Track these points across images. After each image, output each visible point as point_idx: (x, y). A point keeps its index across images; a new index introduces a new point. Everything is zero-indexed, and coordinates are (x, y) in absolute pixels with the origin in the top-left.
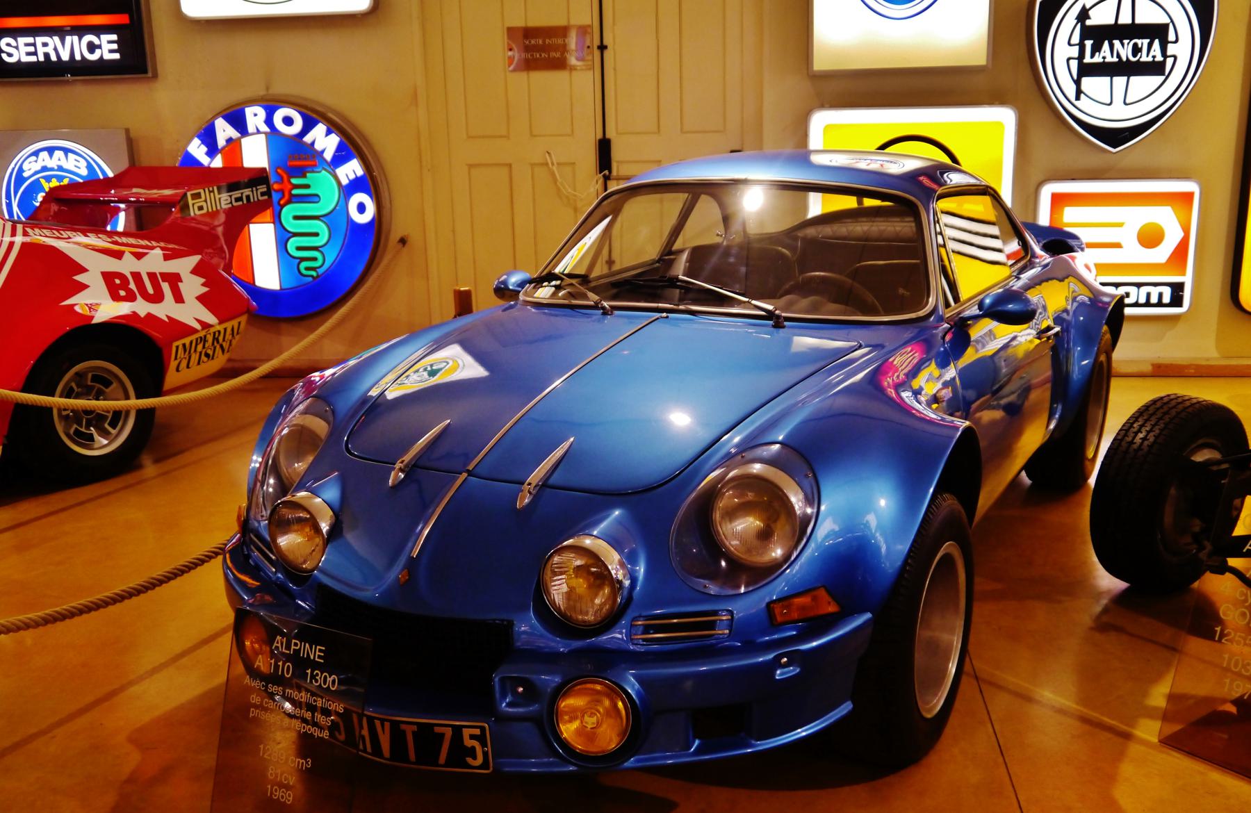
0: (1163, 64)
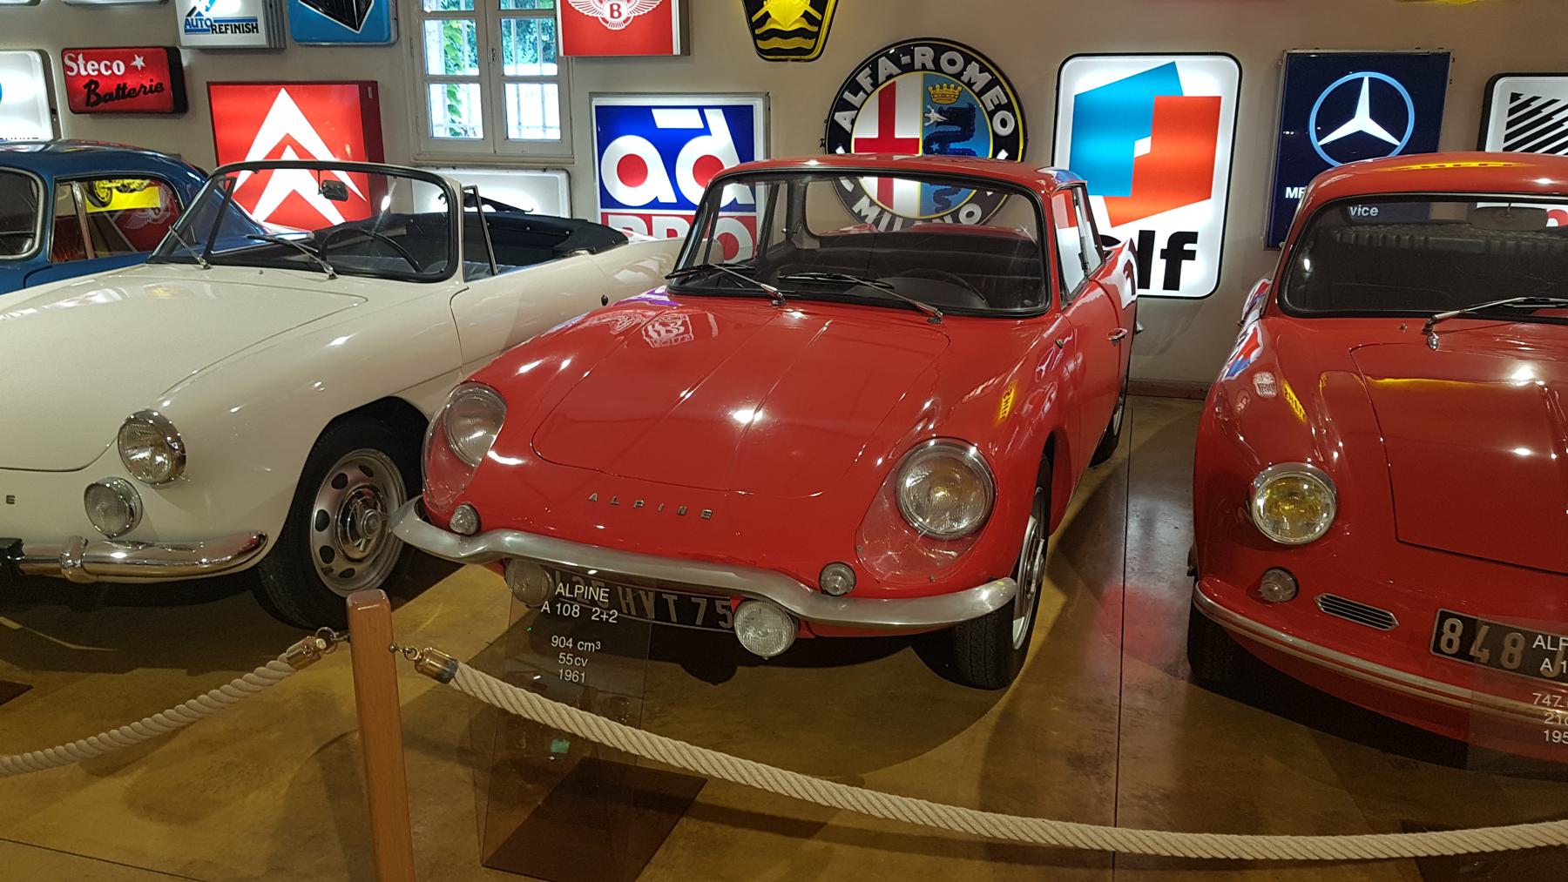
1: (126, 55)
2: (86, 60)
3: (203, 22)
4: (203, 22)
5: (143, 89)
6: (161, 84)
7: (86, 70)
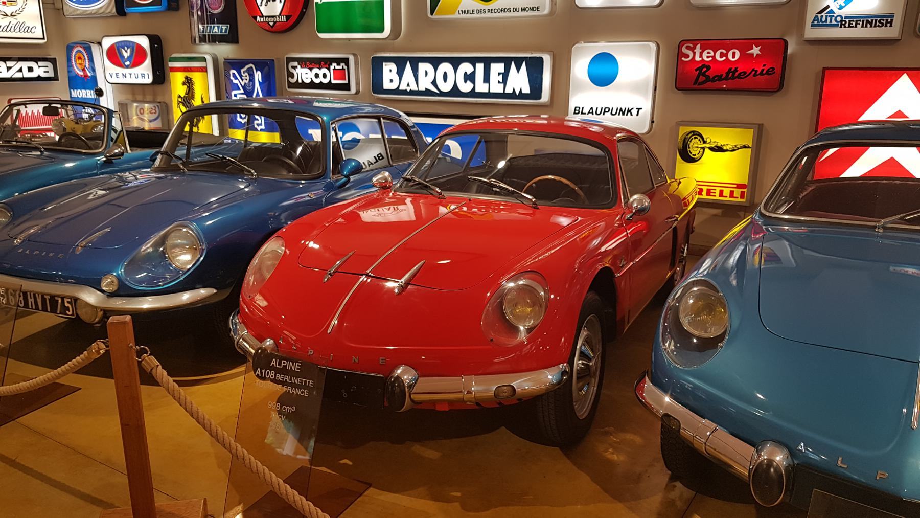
1: (744, 45)
2: (703, 49)
3: (833, 18)
4: (833, 18)
5: (754, 72)
6: (773, 69)
7: (701, 56)
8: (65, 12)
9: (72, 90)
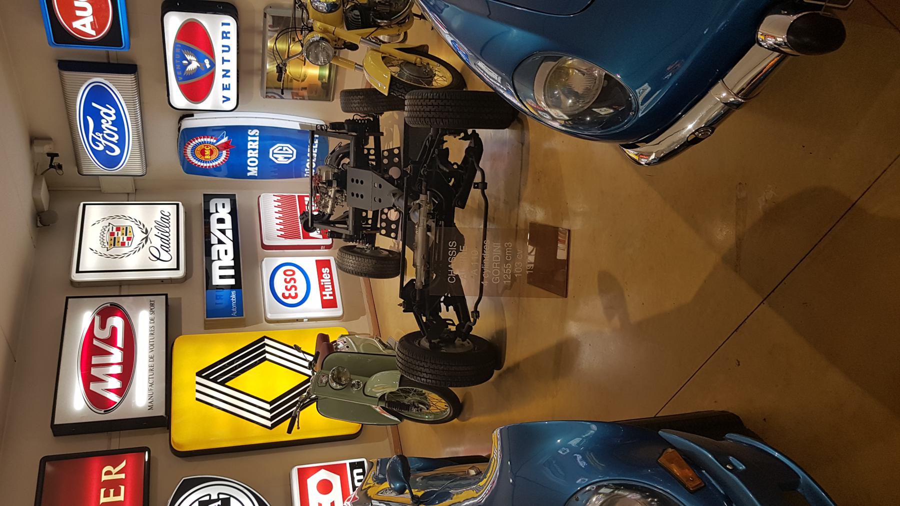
0: (222, 499)
8: (140, 173)
9: (249, 174)
